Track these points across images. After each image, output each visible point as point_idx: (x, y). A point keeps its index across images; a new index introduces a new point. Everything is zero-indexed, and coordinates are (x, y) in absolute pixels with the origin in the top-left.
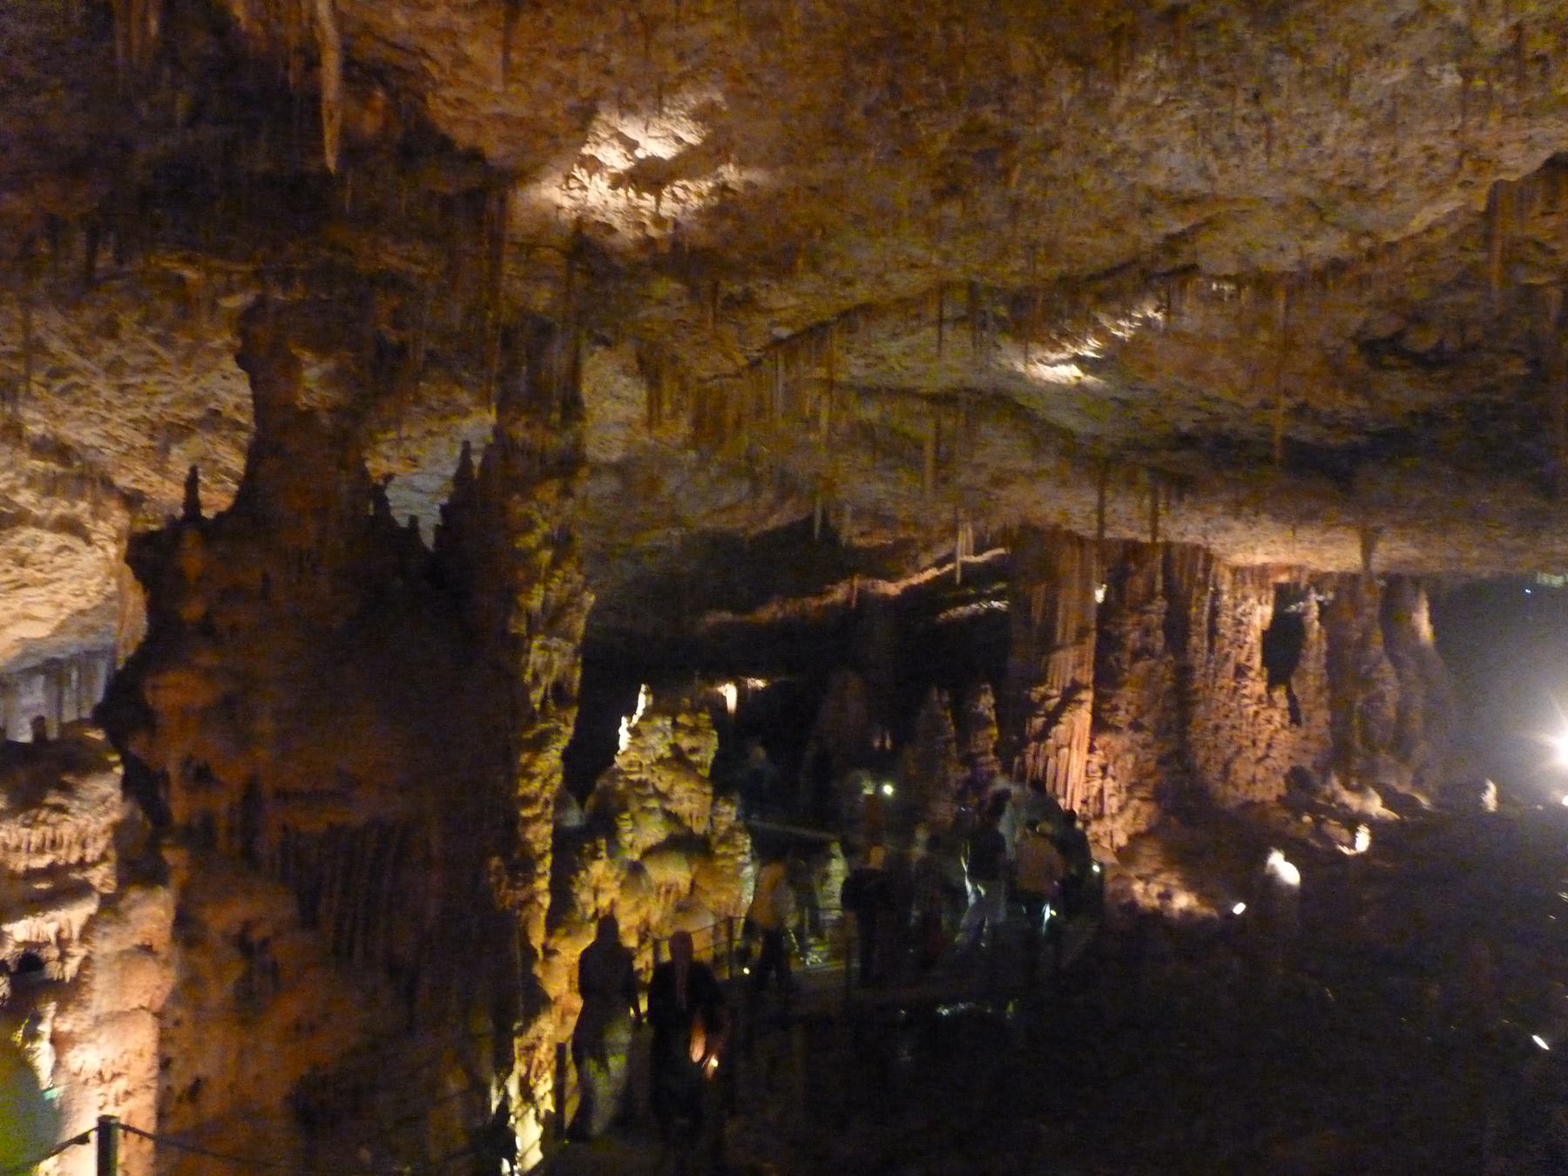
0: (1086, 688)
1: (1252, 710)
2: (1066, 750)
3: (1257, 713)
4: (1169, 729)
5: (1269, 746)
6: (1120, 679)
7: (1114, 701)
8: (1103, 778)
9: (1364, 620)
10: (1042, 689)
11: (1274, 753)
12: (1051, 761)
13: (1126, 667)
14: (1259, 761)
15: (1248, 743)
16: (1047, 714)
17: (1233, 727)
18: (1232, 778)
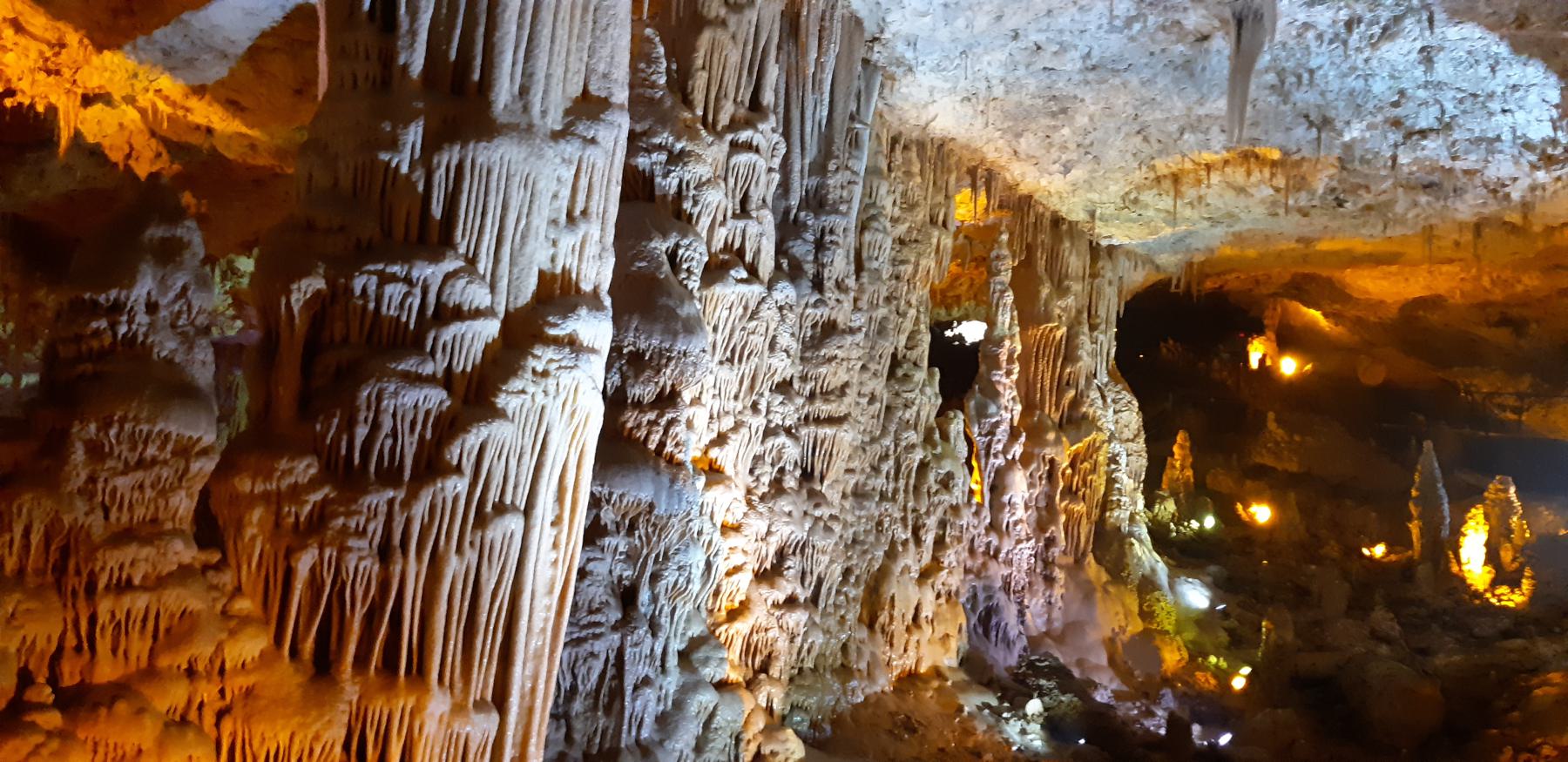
0: (594, 301)
1: (918, 455)
2: (514, 523)
3: (923, 466)
4: (777, 487)
5: (940, 543)
6: (685, 311)
7: (666, 378)
8: (625, 623)
9: (1070, 300)
10: (430, 272)
11: (950, 557)
12: (454, 566)
13: (694, 284)
14: (925, 575)
15: (904, 534)
16: (448, 380)
17: (883, 496)
18: (883, 618)
